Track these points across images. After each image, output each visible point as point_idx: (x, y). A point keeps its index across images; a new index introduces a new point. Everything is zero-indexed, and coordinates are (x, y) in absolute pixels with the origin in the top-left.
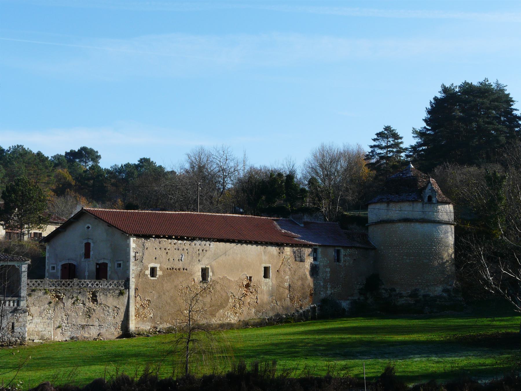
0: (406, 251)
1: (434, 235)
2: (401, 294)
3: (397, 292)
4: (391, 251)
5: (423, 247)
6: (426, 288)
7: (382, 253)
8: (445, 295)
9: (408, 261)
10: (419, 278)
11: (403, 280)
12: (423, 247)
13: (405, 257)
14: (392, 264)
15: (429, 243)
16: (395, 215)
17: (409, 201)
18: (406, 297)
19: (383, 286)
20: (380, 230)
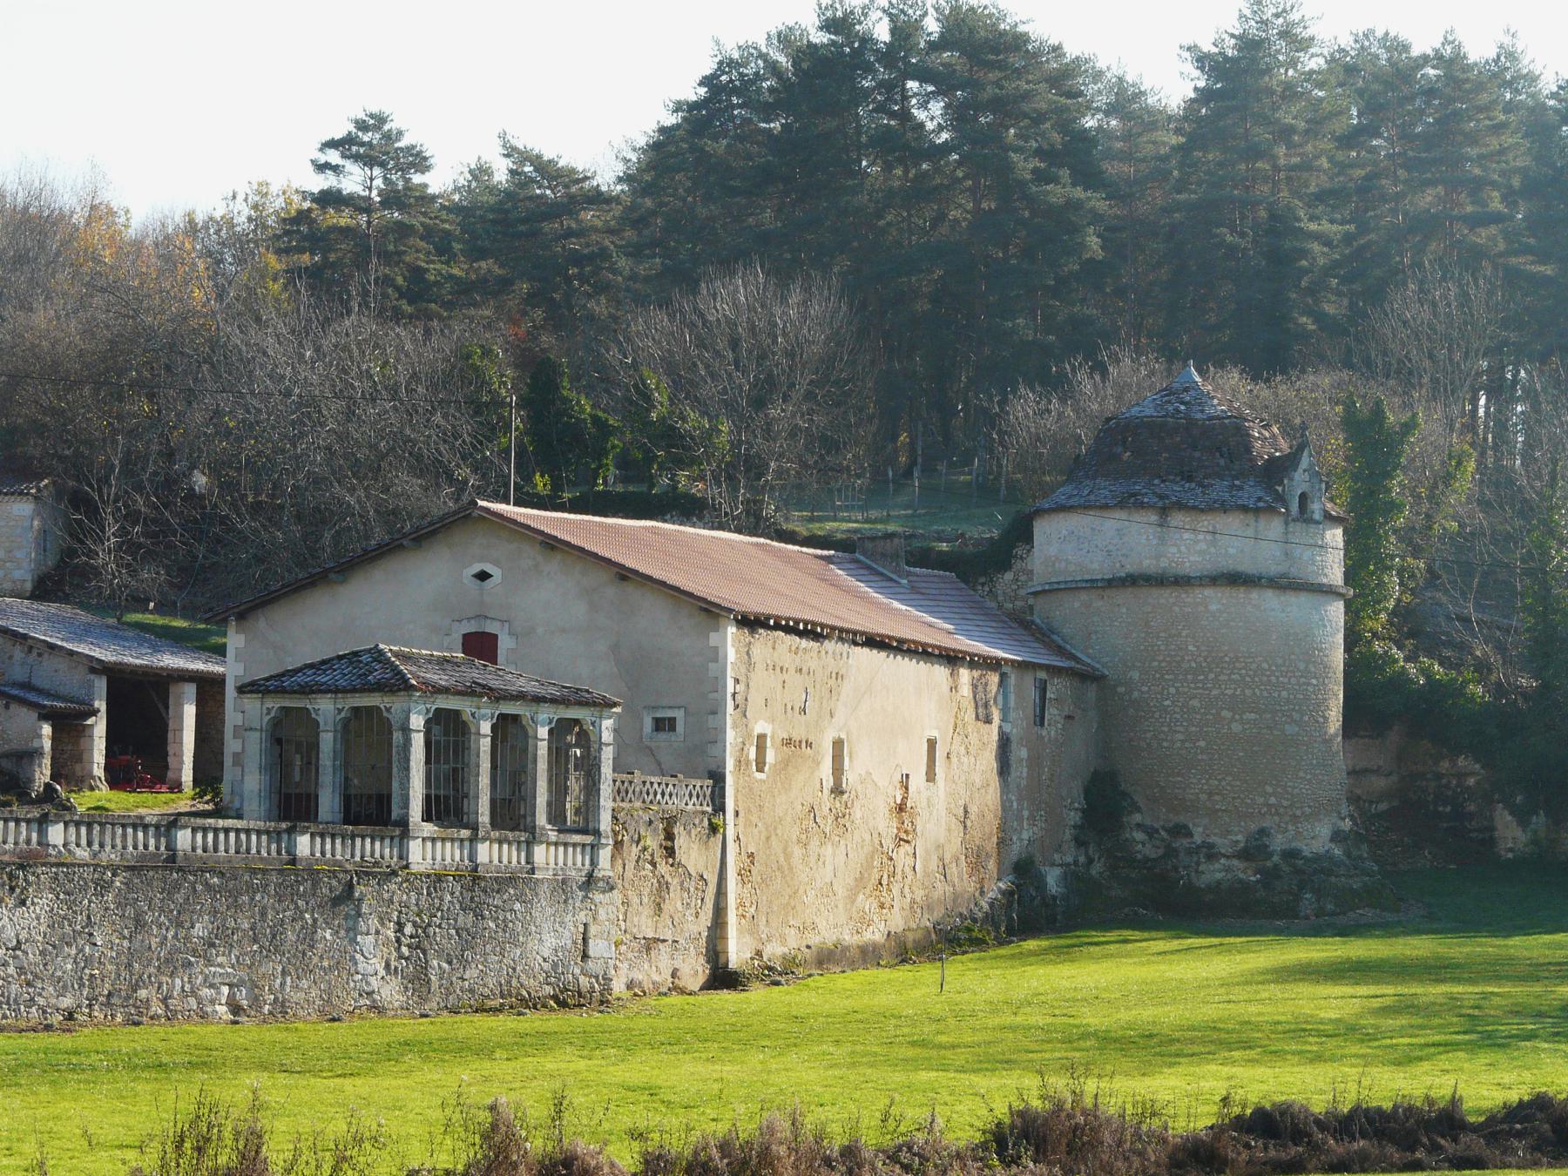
0: (1229, 692)
1: (1314, 635)
2: (1211, 846)
3: (1198, 839)
4: (1172, 690)
5: (1286, 680)
6: (1290, 827)
7: (1136, 694)
8: (1336, 851)
9: (1236, 727)
10: (1269, 789)
11: (1217, 798)
12: (1286, 680)
13: (1225, 713)
14: (1180, 737)
15: (1302, 666)
16: (1192, 558)
17: (1245, 509)
18: (1228, 857)
19: (1137, 818)
20: (1124, 610)
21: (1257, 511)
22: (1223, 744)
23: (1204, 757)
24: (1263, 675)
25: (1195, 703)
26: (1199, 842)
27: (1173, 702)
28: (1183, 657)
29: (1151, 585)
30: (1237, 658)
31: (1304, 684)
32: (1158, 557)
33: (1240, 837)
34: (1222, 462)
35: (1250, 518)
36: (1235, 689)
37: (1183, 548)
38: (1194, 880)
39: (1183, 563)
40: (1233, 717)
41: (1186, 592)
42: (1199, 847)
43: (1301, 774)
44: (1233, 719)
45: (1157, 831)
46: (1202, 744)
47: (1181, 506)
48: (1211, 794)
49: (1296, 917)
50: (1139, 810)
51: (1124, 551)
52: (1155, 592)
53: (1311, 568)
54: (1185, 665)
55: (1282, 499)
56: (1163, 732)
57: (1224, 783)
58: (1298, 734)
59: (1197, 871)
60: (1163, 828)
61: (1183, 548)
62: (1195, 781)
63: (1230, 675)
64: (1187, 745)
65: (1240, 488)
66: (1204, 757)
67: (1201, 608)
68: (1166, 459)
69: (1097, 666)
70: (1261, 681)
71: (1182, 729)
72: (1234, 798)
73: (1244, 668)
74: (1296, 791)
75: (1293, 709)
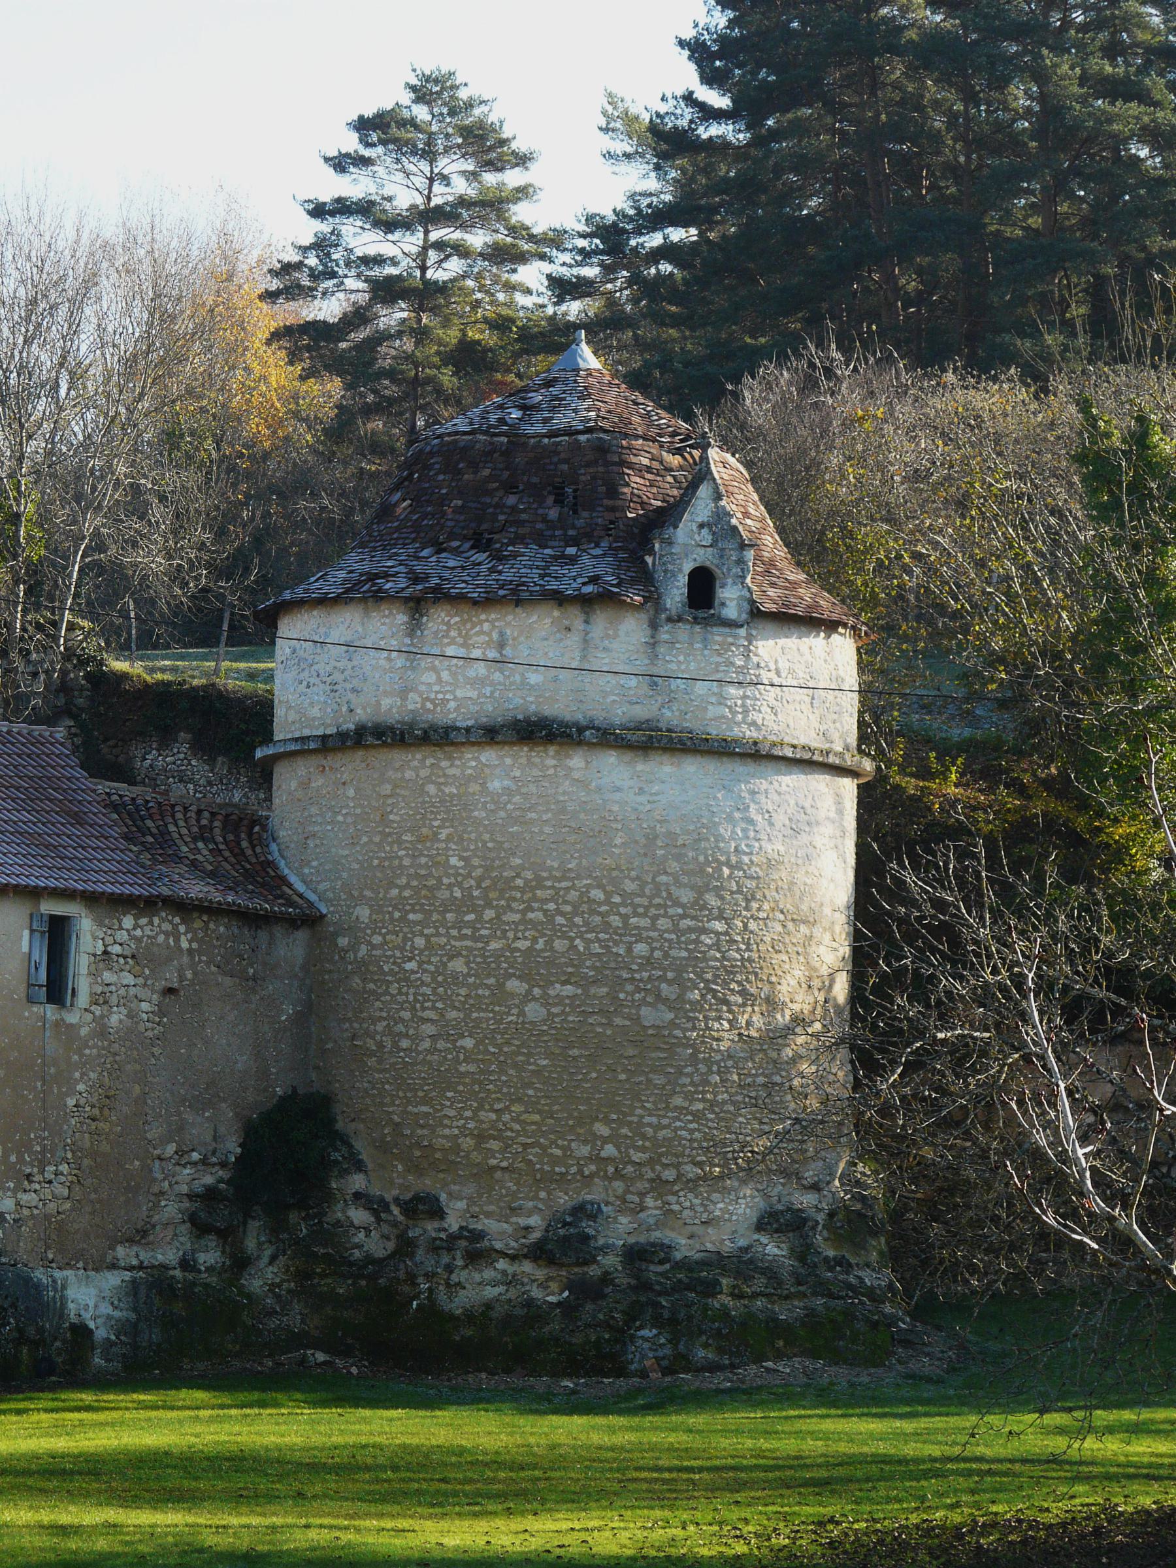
0: (522, 945)
1: (719, 838)
2: (477, 1236)
3: (453, 1223)
4: (420, 942)
5: (644, 922)
6: (649, 1202)
7: (363, 950)
8: (772, 1249)
9: (534, 1011)
10: (602, 1129)
11: (494, 1145)
12: (644, 922)
13: (513, 985)
14: (430, 1029)
15: (686, 896)
16: (459, 693)
17: (559, 599)
18: (513, 1258)
19: (357, 1182)
20: (351, 793)
21: (586, 602)
22: (508, 1043)
23: (472, 1068)
24: (593, 912)
25: (458, 965)
26: (455, 1228)
27: (420, 964)
28: (439, 880)
29: (391, 746)
30: (539, 882)
31: (690, 930)
32: (404, 693)
33: (535, 1221)
34: (553, 514)
35: (574, 616)
36: (535, 940)
37: (445, 675)
38: (442, 1295)
39: (445, 701)
40: (529, 992)
41: (450, 758)
42: (453, 1238)
43: (678, 1101)
44: (528, 997)
45: (386, 1207)
46: (468, 1043)
47: (440, 596)
48: (481, 1138)
49: (621, 1371)
50: (360, 1166)
51: (355, 683)
52: (398, 756)
53: (712, 711)
54: (444, 894)
55: (645, 580)
56: (402, 1020)
57: (506, 1117)
58: (673, 1024)
59: (448, 1285)
60: (396, 1200)
61: (445, 675)
62: (452, 1113)
63: (524, 912)
64: (441, 1045)
65: (573, 560)
66: (472, 1068)
67: (474, 788)
68: (457, 510)
69: (313, 897)
70: (586, 923)
71: (431, 1014)
72: (525, 1146)
73: (552, 899)
74: (662, 1134)
75: (662, 978)
